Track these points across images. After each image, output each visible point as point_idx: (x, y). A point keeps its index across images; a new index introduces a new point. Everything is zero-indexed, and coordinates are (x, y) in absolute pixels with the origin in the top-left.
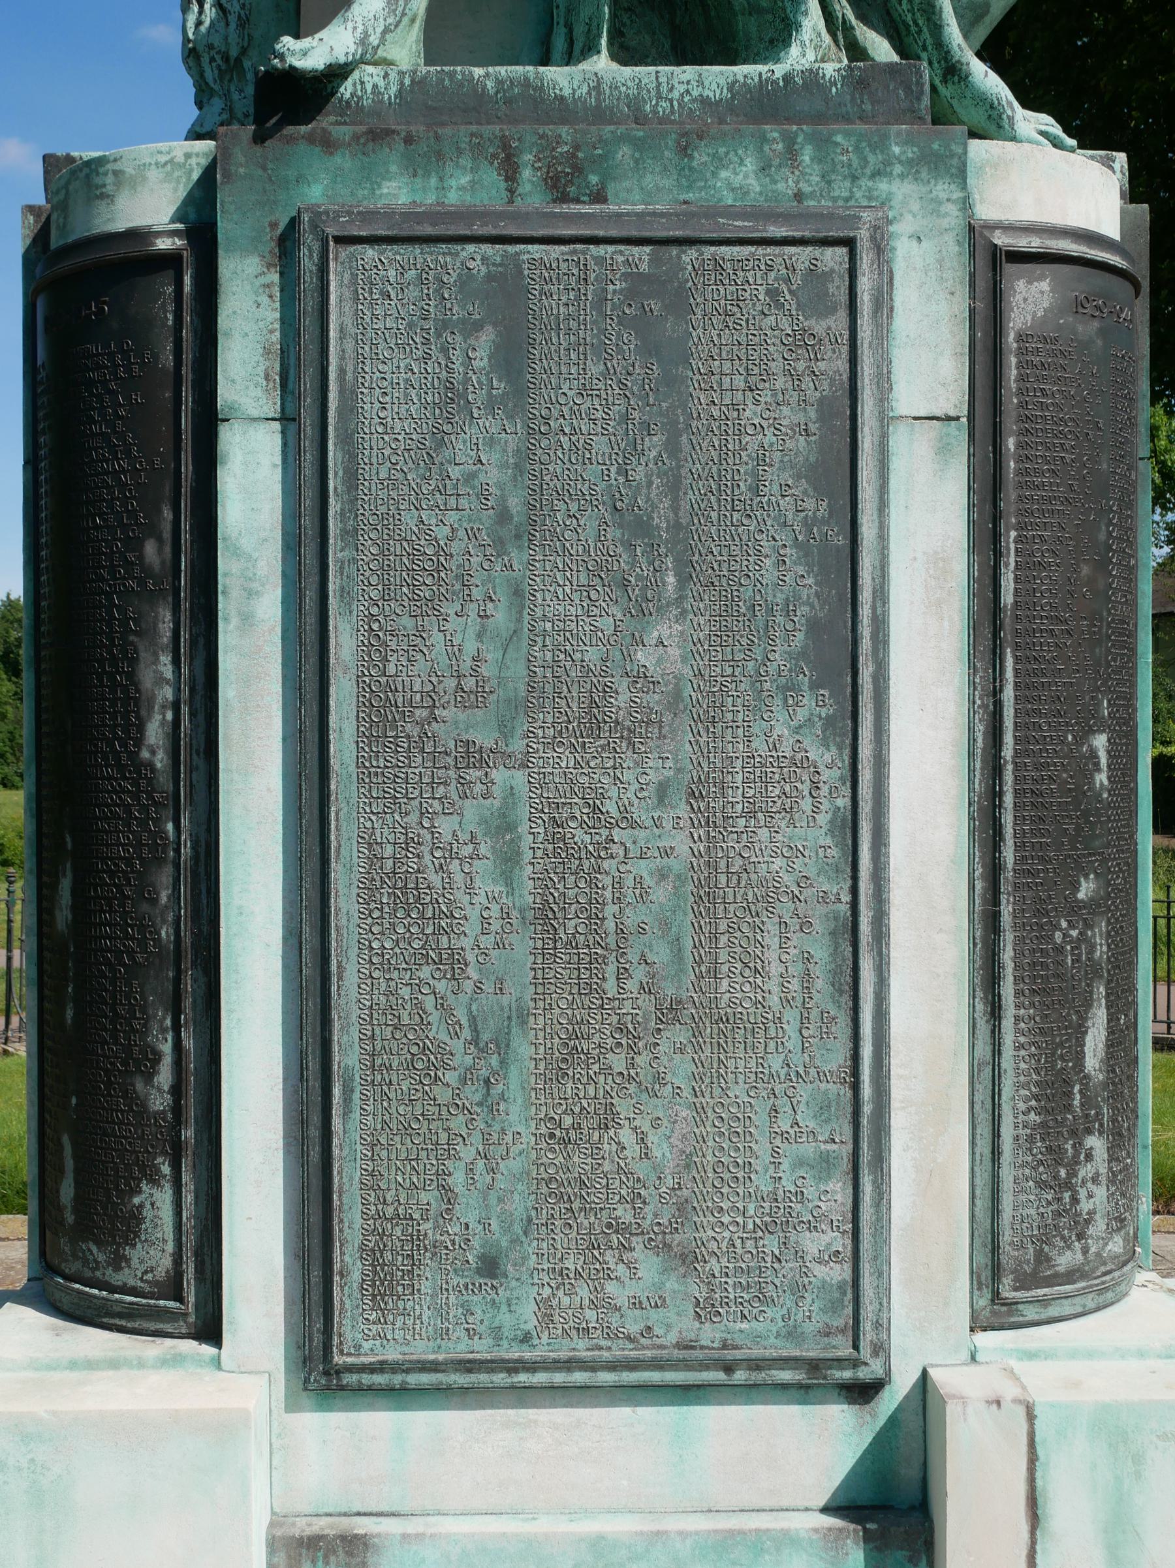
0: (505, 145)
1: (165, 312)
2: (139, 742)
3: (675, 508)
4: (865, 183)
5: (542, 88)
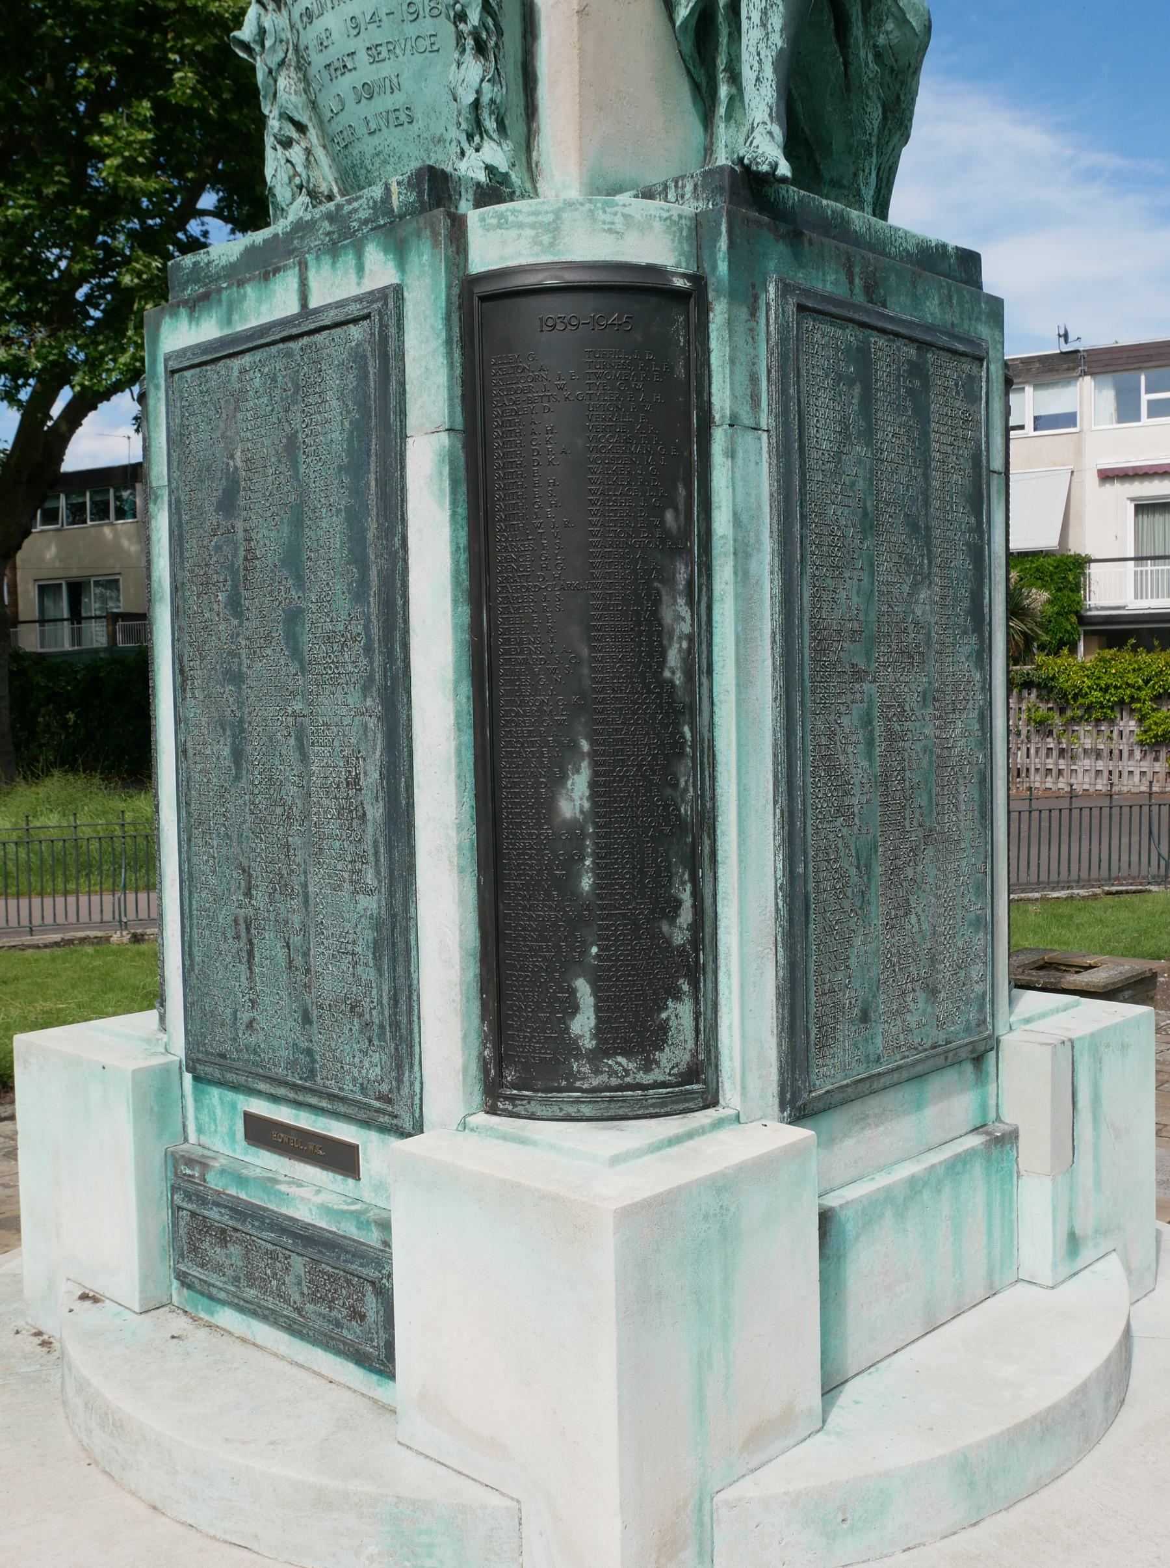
0: (849, 259)
1: (678, 335)
2: (662, 664)
3: (926, 515)
4: (973, 322)
5: (848, 222)
